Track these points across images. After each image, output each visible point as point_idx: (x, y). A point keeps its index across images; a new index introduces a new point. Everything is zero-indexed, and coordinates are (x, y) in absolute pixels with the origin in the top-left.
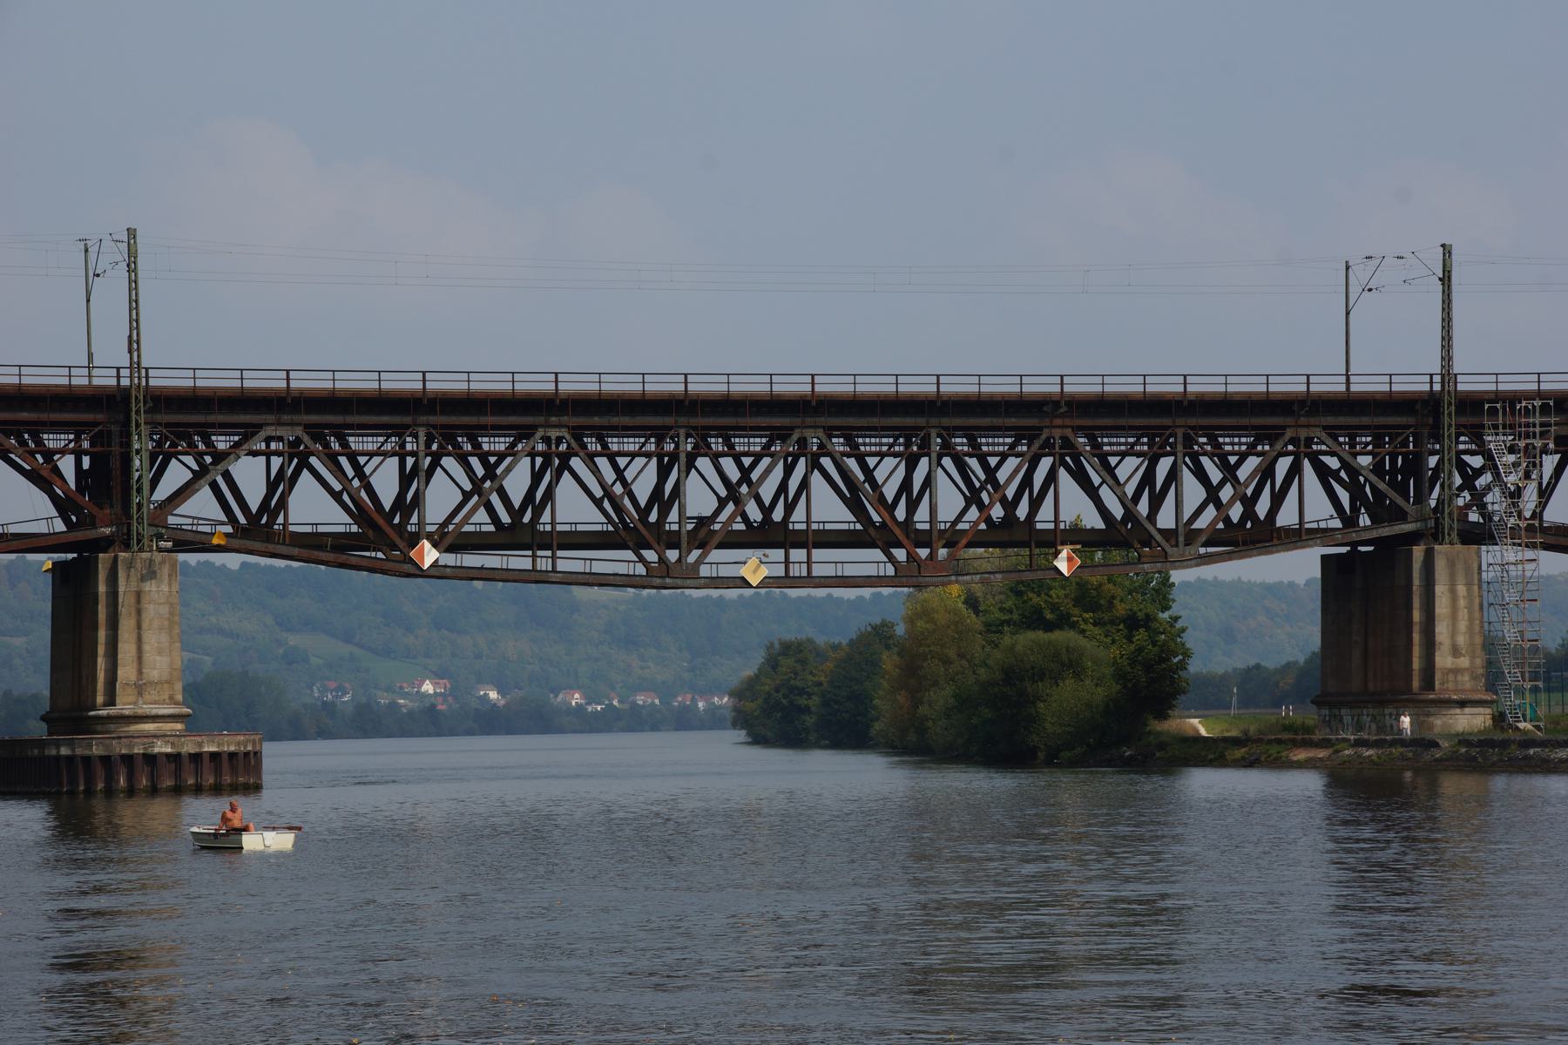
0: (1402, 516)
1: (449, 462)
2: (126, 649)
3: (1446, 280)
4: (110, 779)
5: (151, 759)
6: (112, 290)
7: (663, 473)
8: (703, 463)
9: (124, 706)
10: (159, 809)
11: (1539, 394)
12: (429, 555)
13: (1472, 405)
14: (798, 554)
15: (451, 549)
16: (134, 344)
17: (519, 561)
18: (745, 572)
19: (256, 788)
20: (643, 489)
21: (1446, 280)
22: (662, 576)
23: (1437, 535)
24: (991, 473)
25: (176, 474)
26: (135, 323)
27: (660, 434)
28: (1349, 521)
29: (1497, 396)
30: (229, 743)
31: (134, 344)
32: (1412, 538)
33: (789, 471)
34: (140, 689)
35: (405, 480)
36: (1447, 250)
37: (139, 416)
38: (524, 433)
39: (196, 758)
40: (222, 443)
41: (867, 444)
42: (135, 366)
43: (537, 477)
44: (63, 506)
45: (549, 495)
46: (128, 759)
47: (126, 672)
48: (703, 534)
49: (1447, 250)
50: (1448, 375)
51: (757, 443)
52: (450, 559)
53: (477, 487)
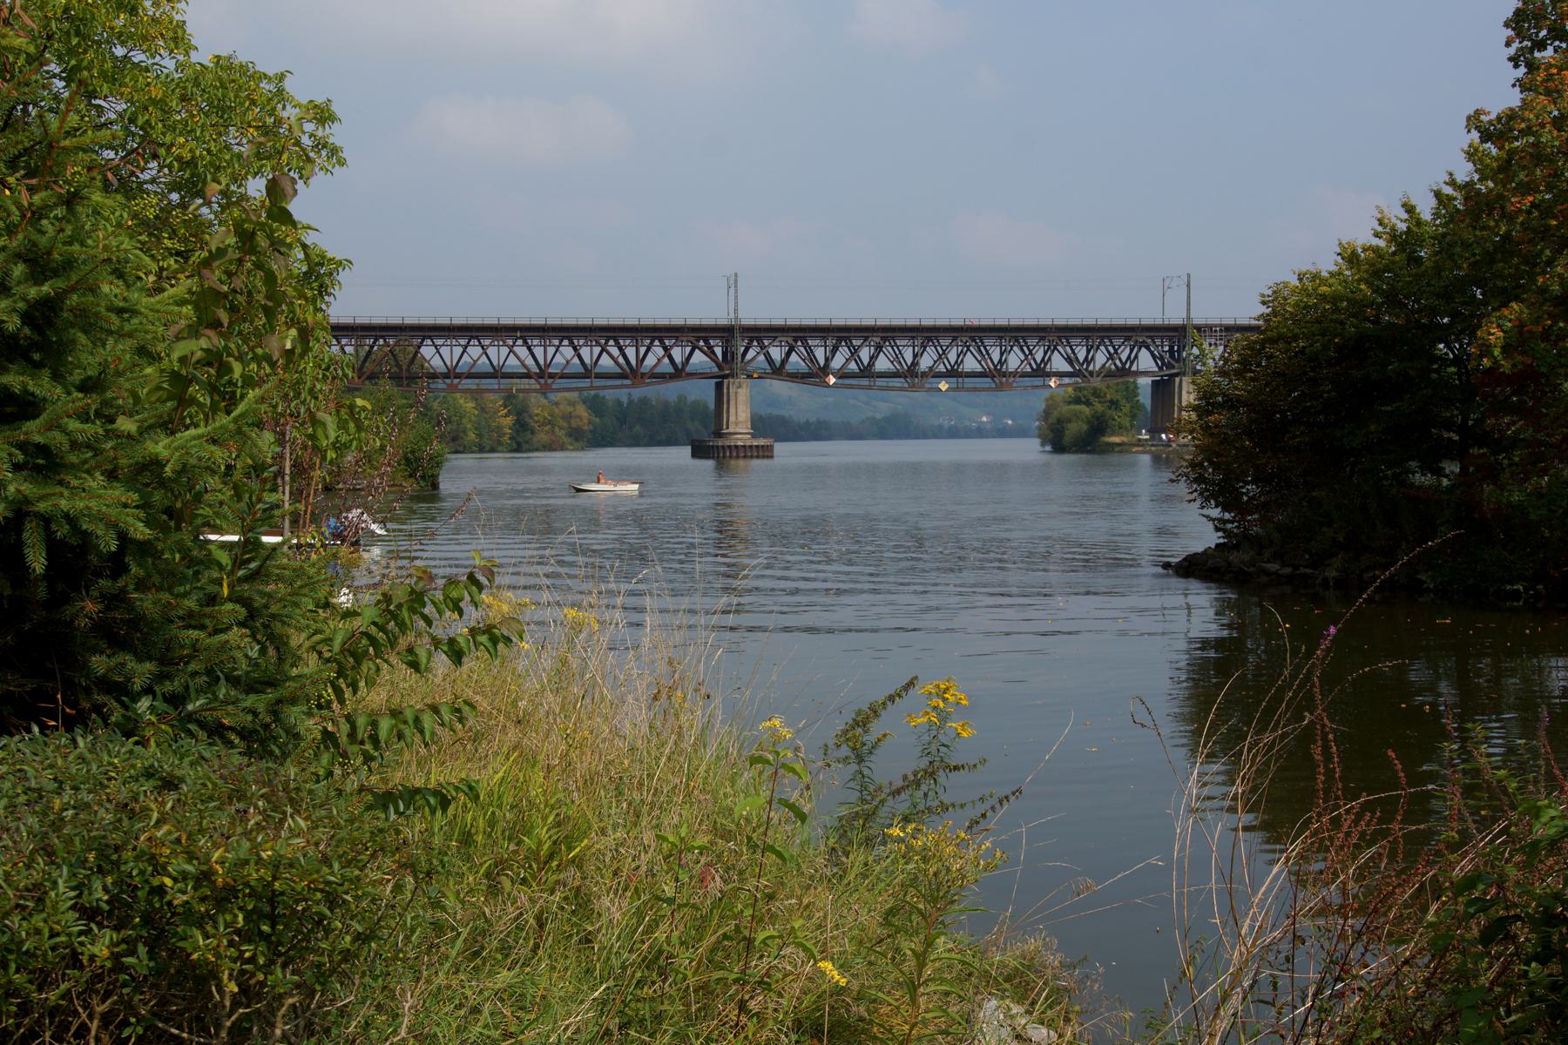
0: (1173, 367)
1: (1015, 348)
2: (732, 410)
3: (1188, 286)
4: (724, 453)
5: (736, 447)
6: (732, 291)
7: (1088, 351)
8: (1102, 348)
9: (731, 430)
10: (741, 462)
11: (1221, 325)
12: (832, 380)
13: (1199, 328)
14: (960, 380)
15: (840, 377)
16: (736, 311)
17: (865, 382)
18: (941, 386)
19: (772, 457)
20: (1081, 356)
21: (1188, 286)
22: (913, 387)
23: (1184, 374)
24: (1030, 351)
25: (751, 354)
26: (736, 303)
27: (1087, 338)
28: (1161, 368)
29: (1206, 326)
30: (761, 442)
31: (736, 311)
32: (1177, 375)
33: (1132, 351)
34: (737, 424)
35: (1002, 354)
36: (1189, 275)
37: (737, 335)
38: (1042, 338)
39: (751, 447)
40: (766, 342)
41: (987, 342)
42: (736, 318)
43: (1045, 353)
44: (719, 366)
45: (1050, 359)
46: (730, 447)
47: (732, 419)
48: (933, 374)
49: (1189, 275)
50: (1188, 318)
51: (947, 342)
52: (840, 381)
53: (1026, 356)
